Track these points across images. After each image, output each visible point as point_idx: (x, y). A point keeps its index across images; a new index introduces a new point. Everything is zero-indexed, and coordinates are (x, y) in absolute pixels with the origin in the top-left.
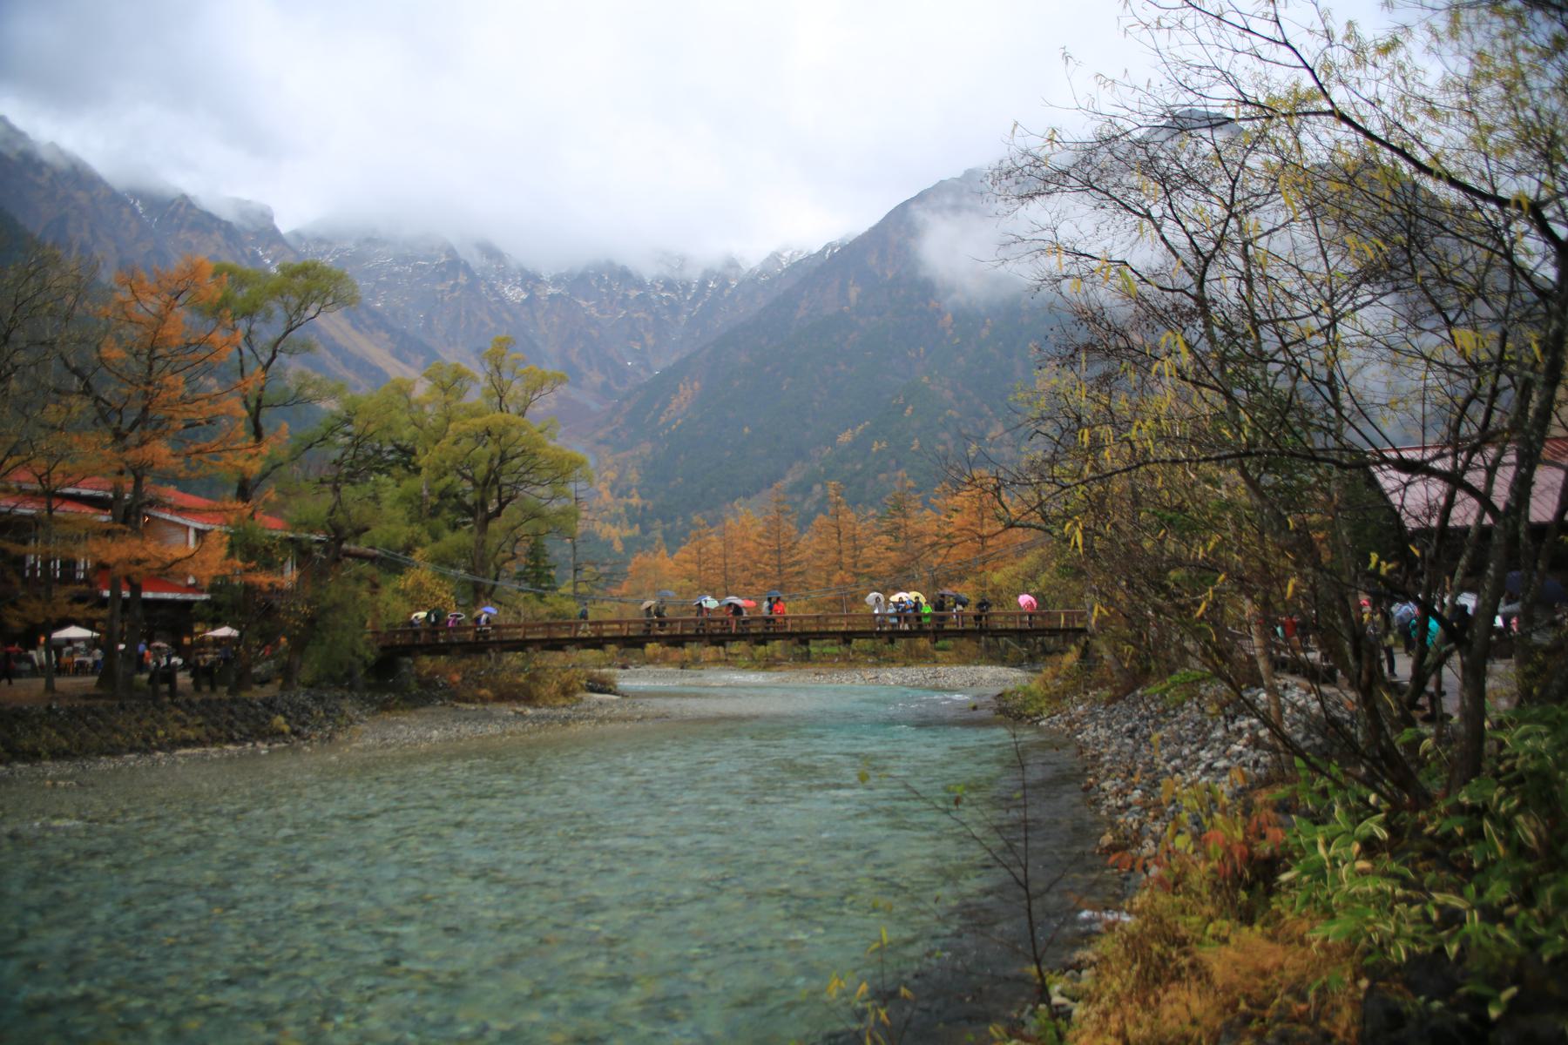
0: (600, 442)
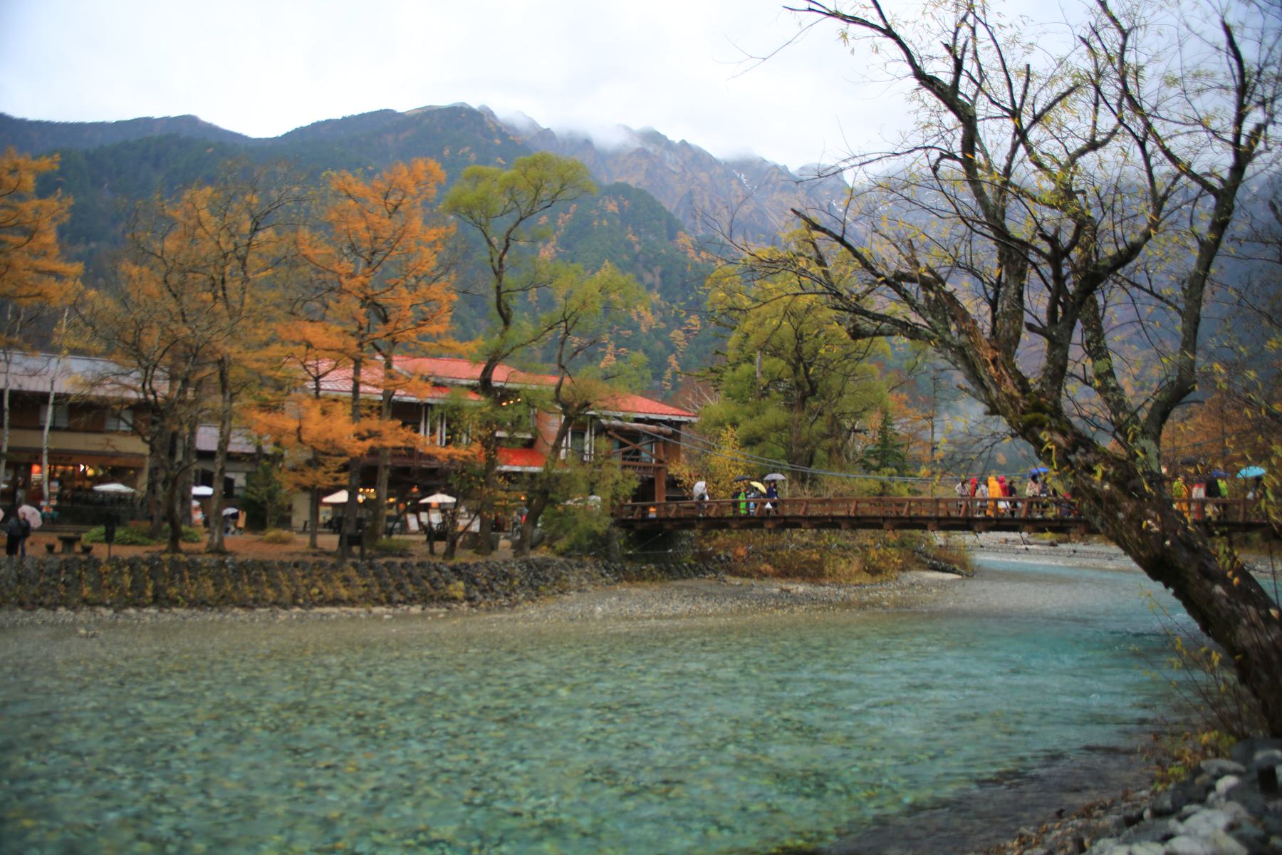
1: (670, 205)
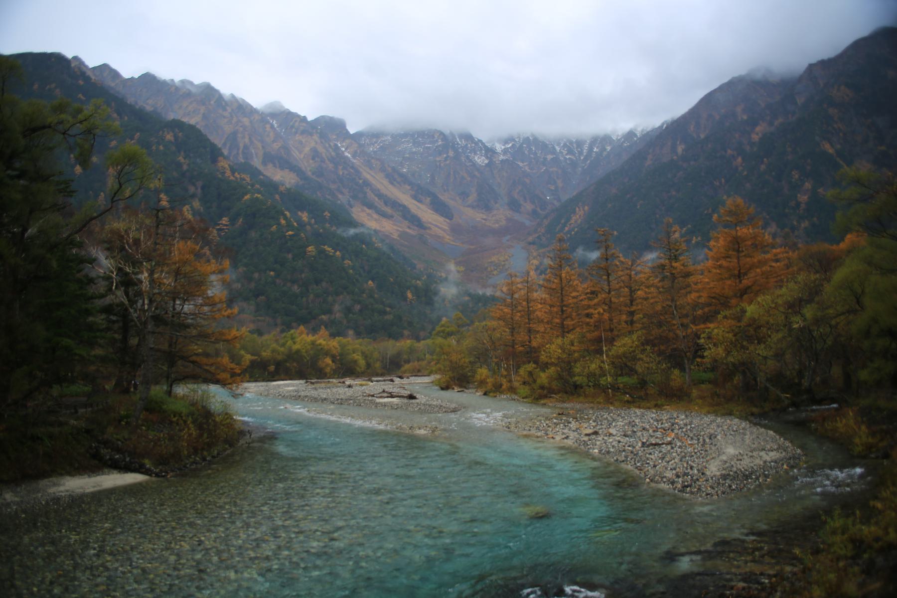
0: (530, 243)
1: (217, 140)
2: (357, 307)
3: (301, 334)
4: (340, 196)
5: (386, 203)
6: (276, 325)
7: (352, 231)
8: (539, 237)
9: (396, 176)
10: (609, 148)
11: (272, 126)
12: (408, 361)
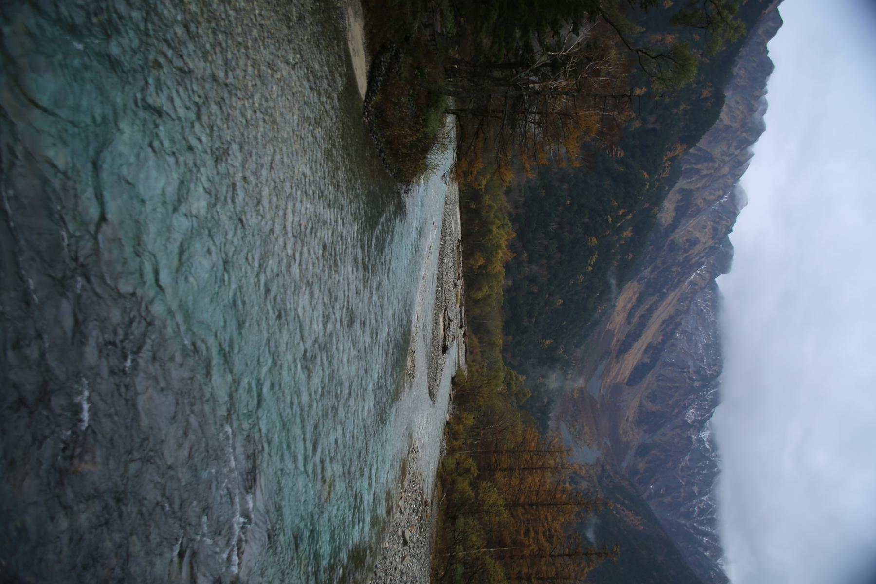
0: (603, 467)
1: (703, 143)
2: (535, 289)
3: (508, 234)
4: (649, 269)
5: (642, 316)
6: (516, 208)
7: (613, 281)
8: (609, 476)
9: (671, 327)
10: (707, 554)
11: (721, 197)
12: (481, 341)
